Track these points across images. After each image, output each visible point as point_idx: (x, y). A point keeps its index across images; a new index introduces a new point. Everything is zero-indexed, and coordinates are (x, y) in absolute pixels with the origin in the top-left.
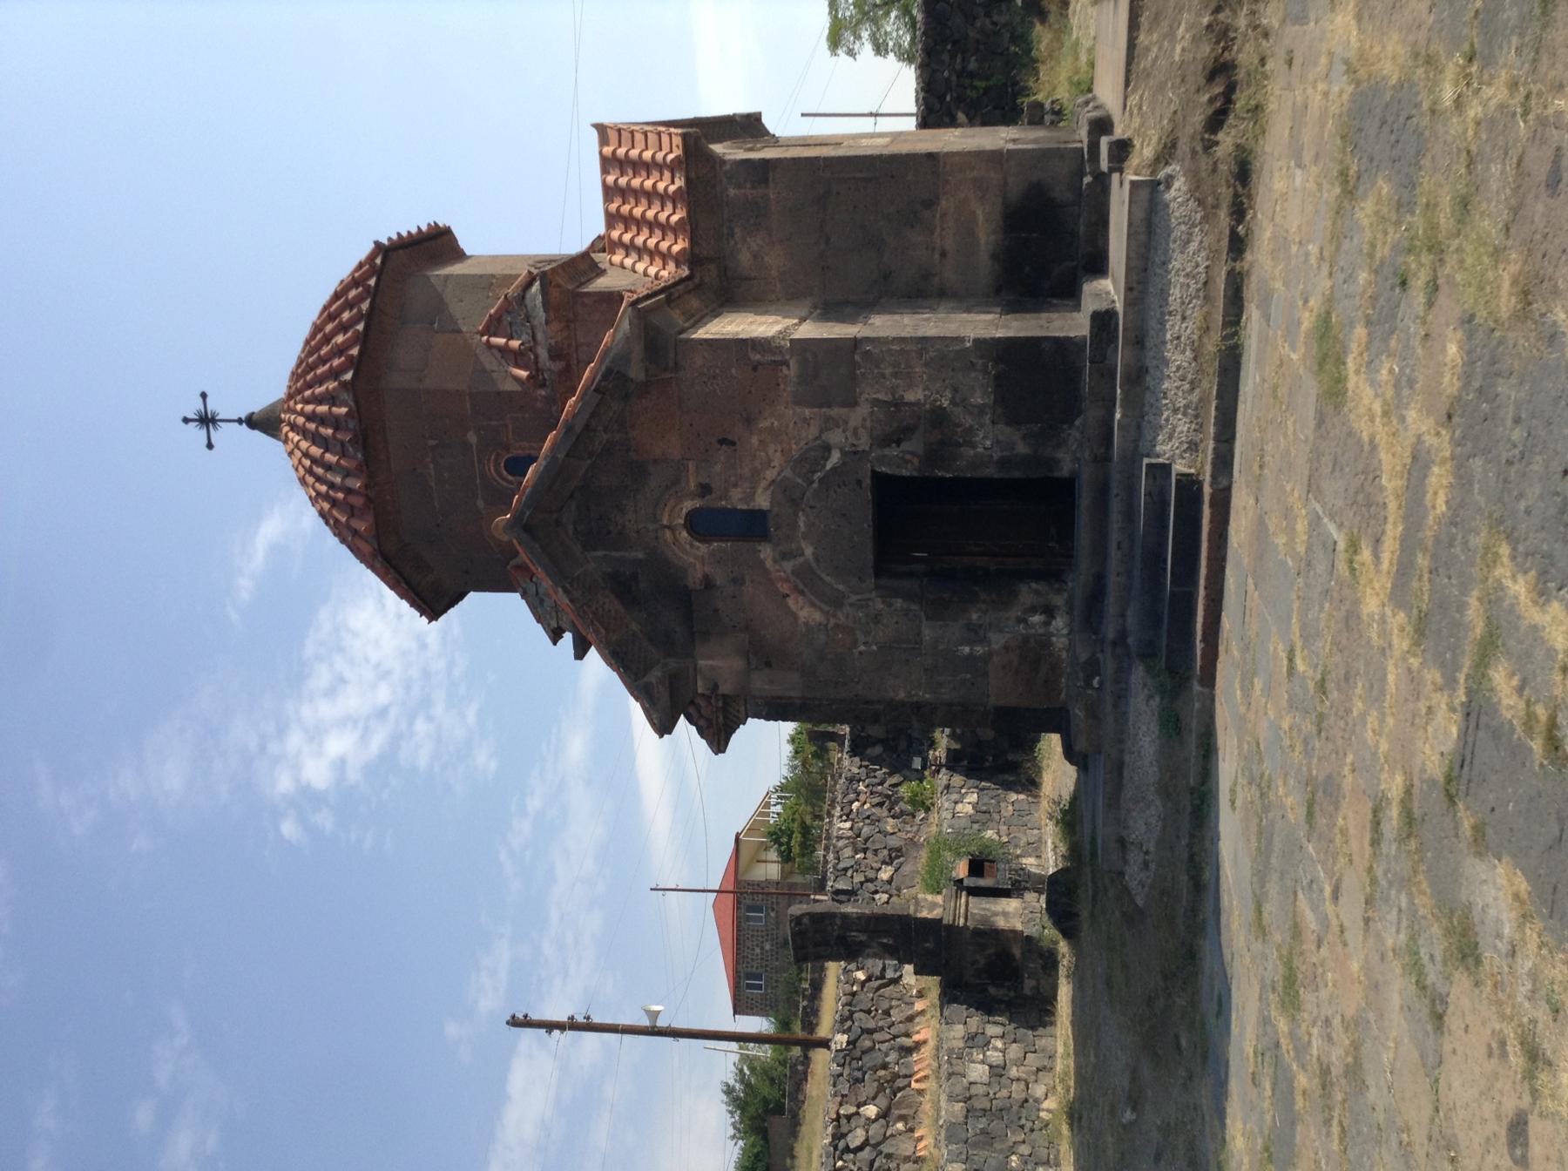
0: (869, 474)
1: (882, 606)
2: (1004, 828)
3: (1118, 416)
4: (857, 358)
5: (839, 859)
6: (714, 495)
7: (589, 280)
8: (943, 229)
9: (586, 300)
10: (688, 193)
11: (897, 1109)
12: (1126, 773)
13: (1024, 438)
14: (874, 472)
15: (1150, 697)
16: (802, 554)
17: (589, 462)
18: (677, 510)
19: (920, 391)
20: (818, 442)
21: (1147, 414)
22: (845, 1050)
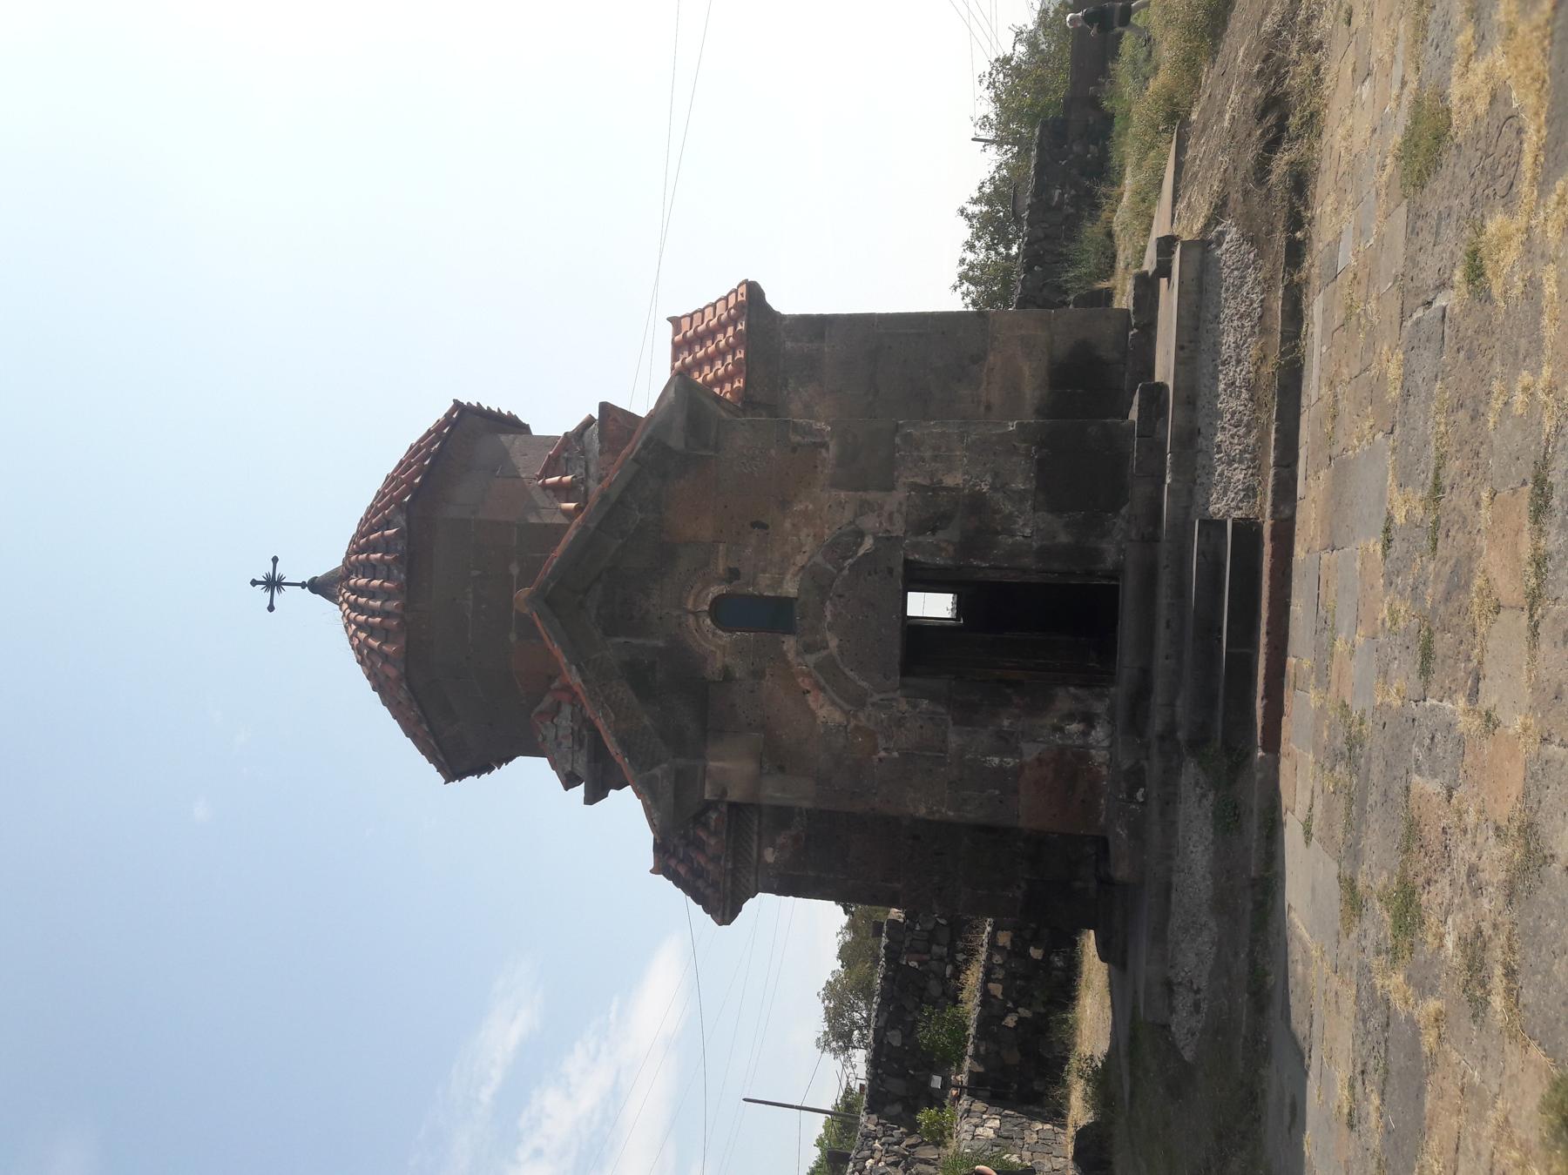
0: (902, 560)
2: (1027, 1154)
3: (1168, 481)
4: (897, 440)
8: (989, 384)
12: (1174, 896)
15: (1204, 796)
16: (827, 647)
17: (620, 541)
19: (959, 476)
20: (853, 526)
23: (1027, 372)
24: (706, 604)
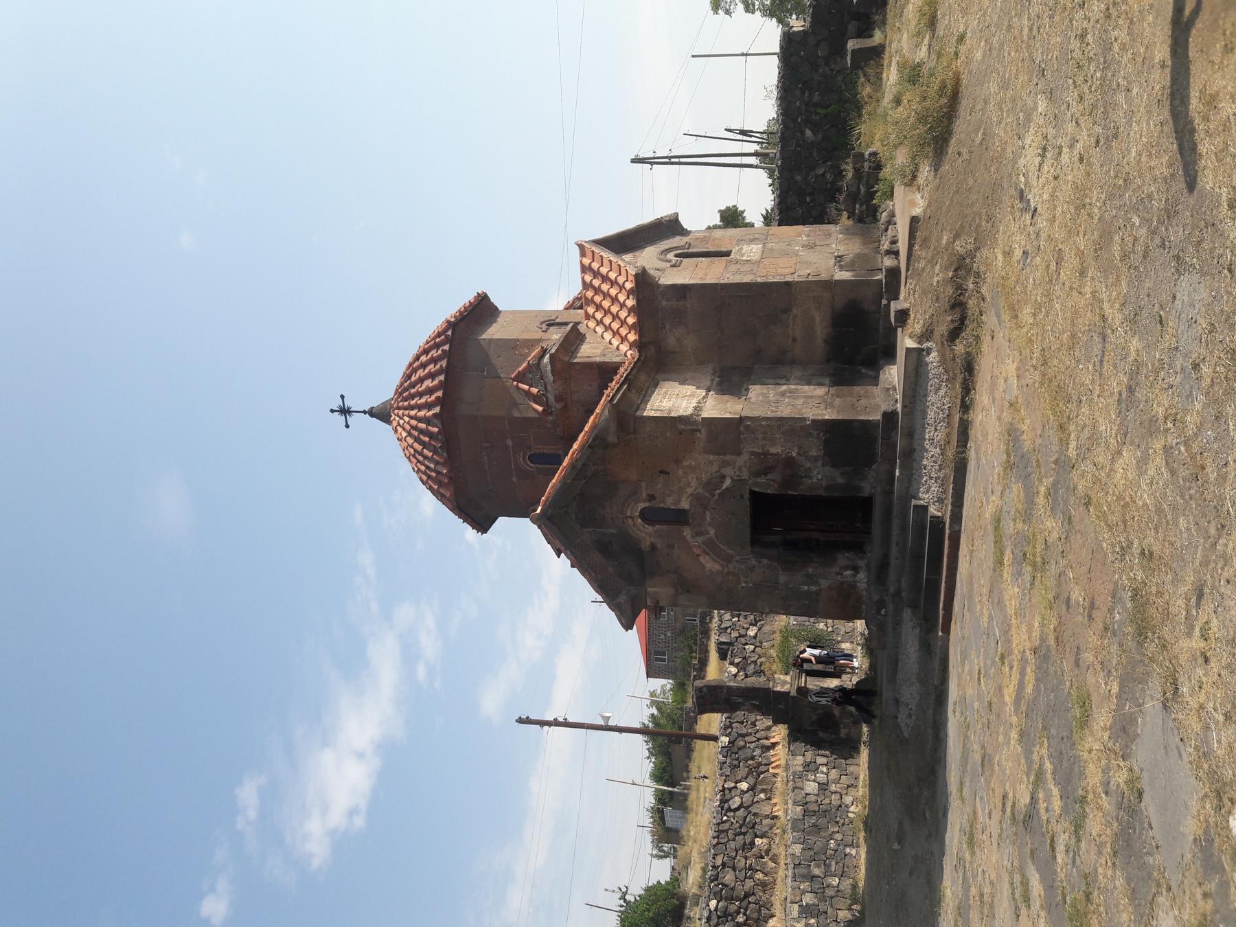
3: (897, 474)
4: (742, 429)
5: (722, 621)
6: (656, 501)
7: (576, 349)
8: (794, 325)
12: (900, 664)
14: (751, 490)
16: (708, 533)
17: (584, 481)
18: (635, 507)
19: (779, 447)
21: (914, 474)
22: (726, 747)
23: (818, 319)
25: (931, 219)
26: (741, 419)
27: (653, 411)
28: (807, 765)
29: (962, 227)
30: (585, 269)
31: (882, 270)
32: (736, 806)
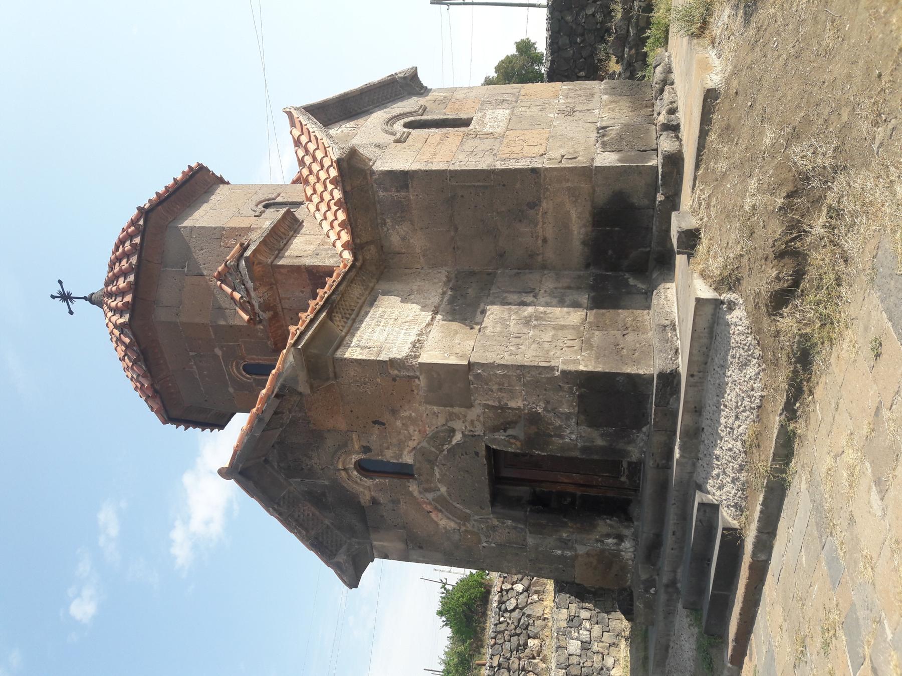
0: (484, 448)
1: (498, 523)
3: (677, 454)
4: (471, 378)
7: (285, 245)
8: (544, 223)
9: (282, 270)
10: (346, 203)
11: (533, 587)
13: (602, 435)
14: (488, 447)
16: (439, 490)
24: (352, 464)
25: (740, 98)
26: (470, 365)
27: (359, 349)
28: (571, 619)
29: (808, 121)
30: (297, 143)
31: (657, 150)
32: (512, 607)
